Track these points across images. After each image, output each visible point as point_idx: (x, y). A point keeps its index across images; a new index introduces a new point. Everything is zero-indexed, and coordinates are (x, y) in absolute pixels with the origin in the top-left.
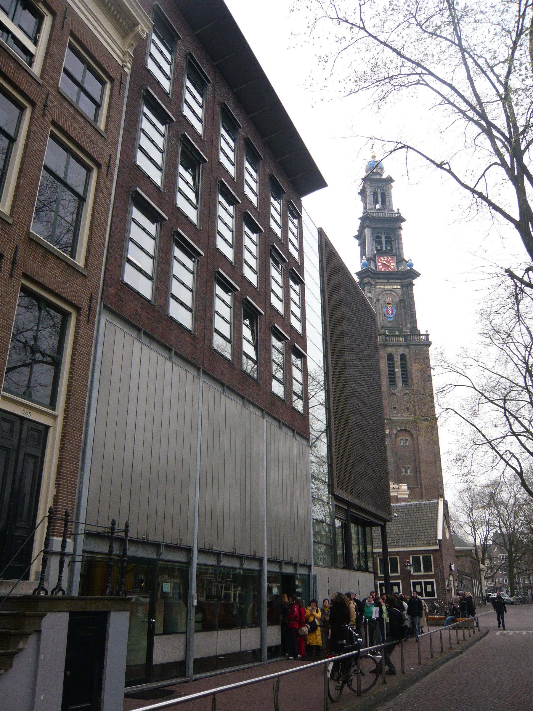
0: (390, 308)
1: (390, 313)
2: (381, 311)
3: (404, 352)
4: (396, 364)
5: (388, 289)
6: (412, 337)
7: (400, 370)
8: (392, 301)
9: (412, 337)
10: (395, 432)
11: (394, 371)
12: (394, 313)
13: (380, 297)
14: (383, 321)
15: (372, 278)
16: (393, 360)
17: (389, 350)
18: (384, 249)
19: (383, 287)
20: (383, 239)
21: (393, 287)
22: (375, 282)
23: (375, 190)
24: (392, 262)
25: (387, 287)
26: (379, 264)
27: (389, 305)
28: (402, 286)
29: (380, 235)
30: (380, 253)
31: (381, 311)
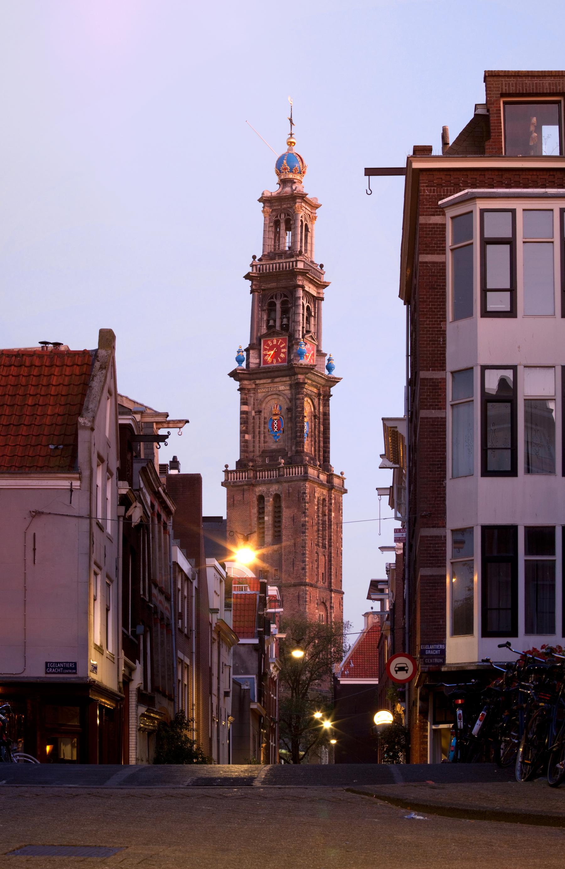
1: (276, 430)
2: (262, 429)
3: (278, 492)
4: (266, 510)
5: (273, 393)
6: (285, 470)
7: (271, 518)
9: (285, 470)
12: (281, 429)
13: (264, 405)
14: (265, 442)
15: (250, 380)
22: (256, 385)
24: (284, 348)
27: (275, 417)
28: (291, 386)
29: (274, 300)
30: (271, 331)
31: (262, 429)
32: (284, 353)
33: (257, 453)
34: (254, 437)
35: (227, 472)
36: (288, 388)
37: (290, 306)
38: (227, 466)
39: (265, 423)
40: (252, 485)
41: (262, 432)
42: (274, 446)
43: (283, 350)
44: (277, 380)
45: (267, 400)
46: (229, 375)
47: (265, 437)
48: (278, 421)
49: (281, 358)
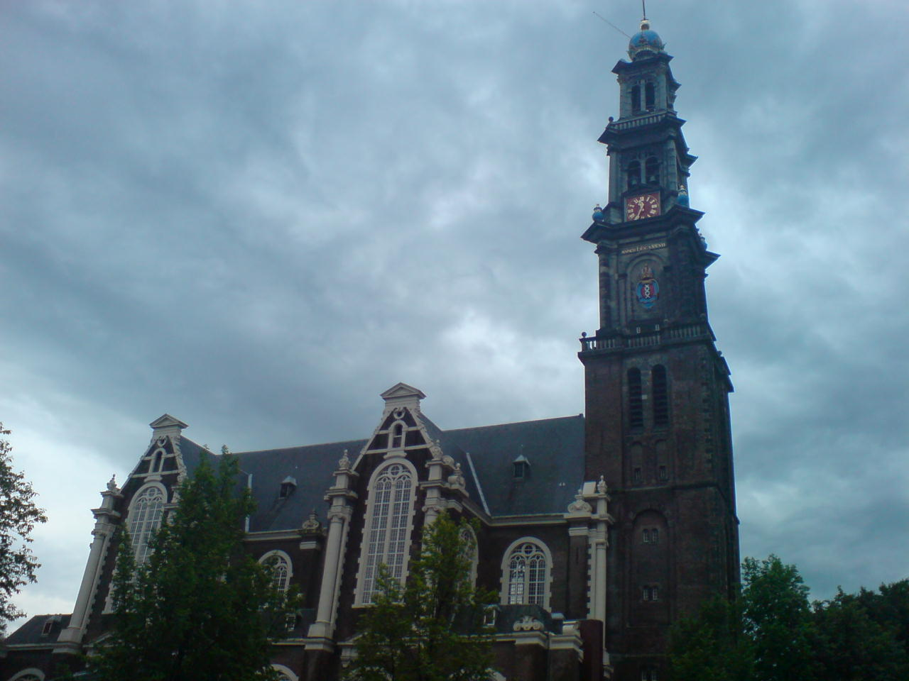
0: (647, 286)
2: (629, 295)
8: (653, 273)
10: (632, 516)
11: (640, 400)
12: (656, 293)
14: (633, 311)
16: (639, 380)
17: (631, 362)
18: (643, 181)
19: (634, 250)
20: (643, 166)
21: (653, 247)
23: (636, 83)
24: (654, 204)
25: (641, 249)
26: (629, 211)
27: (647, 281)
29: (638, 159)
30: (635, 191)
31: (629, 295)
32: (654, 209)
33: (623, 321)
34: (619, 304)
35: (584, 341)
36: (664, 245)
37: (659, 161)
38: (584, 334)
39: (633, 289)
40: (622, 356)
41: (629, 299)
42: (646, 316)
43: (653, 206)
44: (647, 237)
45: (635, 262)
46: (582, 237)
47: (632, 305)
48: (651, 285)
49: (651, 215)
